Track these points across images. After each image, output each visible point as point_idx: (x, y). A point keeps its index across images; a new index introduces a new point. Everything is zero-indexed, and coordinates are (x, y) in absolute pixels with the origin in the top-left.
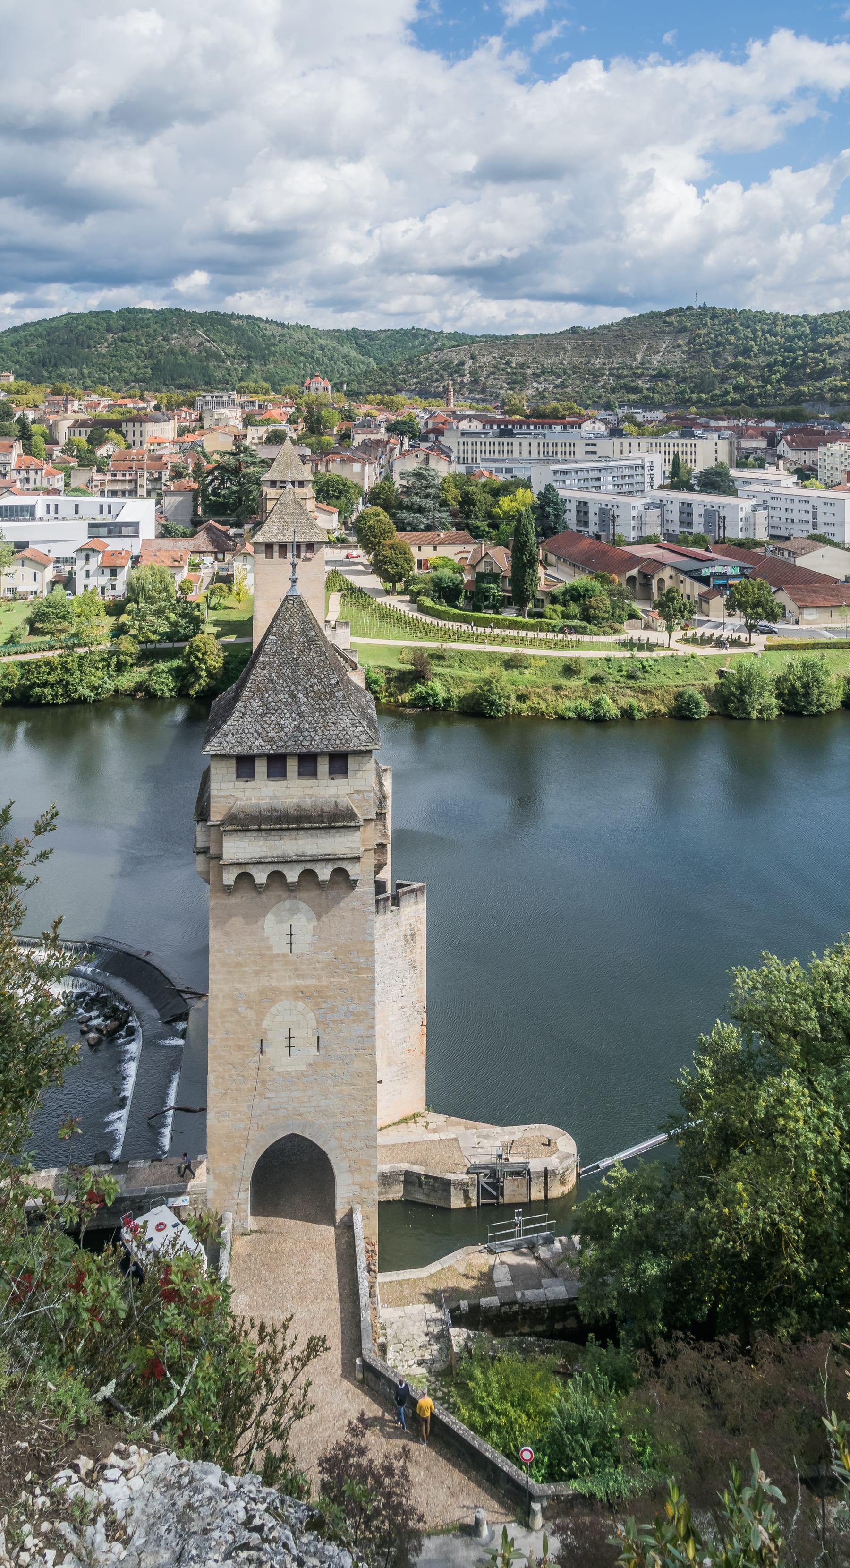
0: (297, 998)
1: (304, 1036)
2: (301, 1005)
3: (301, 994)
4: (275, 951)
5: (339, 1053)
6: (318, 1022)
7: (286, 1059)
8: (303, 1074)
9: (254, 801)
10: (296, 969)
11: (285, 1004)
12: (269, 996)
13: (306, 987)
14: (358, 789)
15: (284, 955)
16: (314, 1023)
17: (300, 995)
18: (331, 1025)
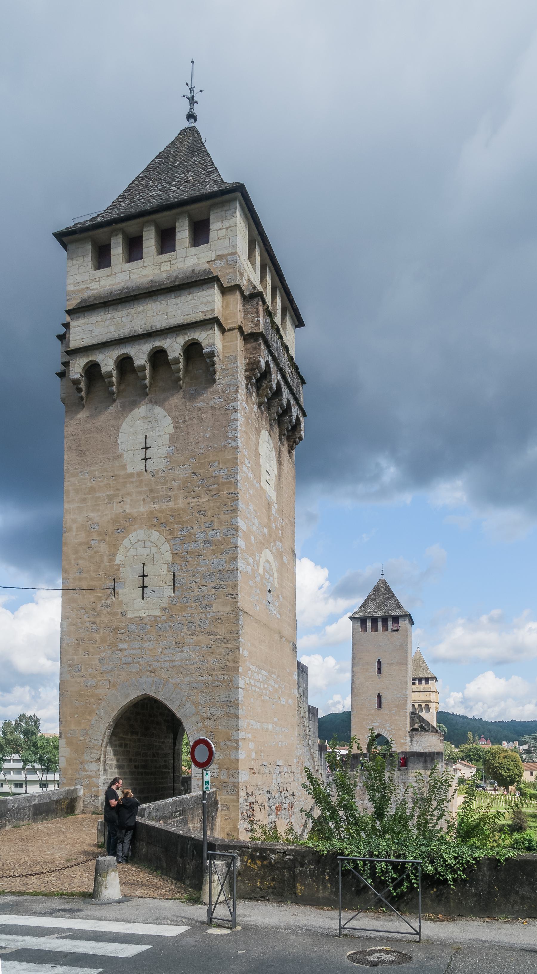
0: (152, 526)
1: (159, 573)
2: (155, 534)
3: (156, 521)
4: (130, 470)
5: (196, 592)
6: (173, 555)
7: (138, 603)
8: (155, 621)
9: (108, 287)
10: (151, 491)
11: (137, 535)
12: (122, 526)
13: (161, 511)
14: (221, 252)
15: (139, 474)
16: (168, 557)
17: (155, 522)
18: (188, 557)
